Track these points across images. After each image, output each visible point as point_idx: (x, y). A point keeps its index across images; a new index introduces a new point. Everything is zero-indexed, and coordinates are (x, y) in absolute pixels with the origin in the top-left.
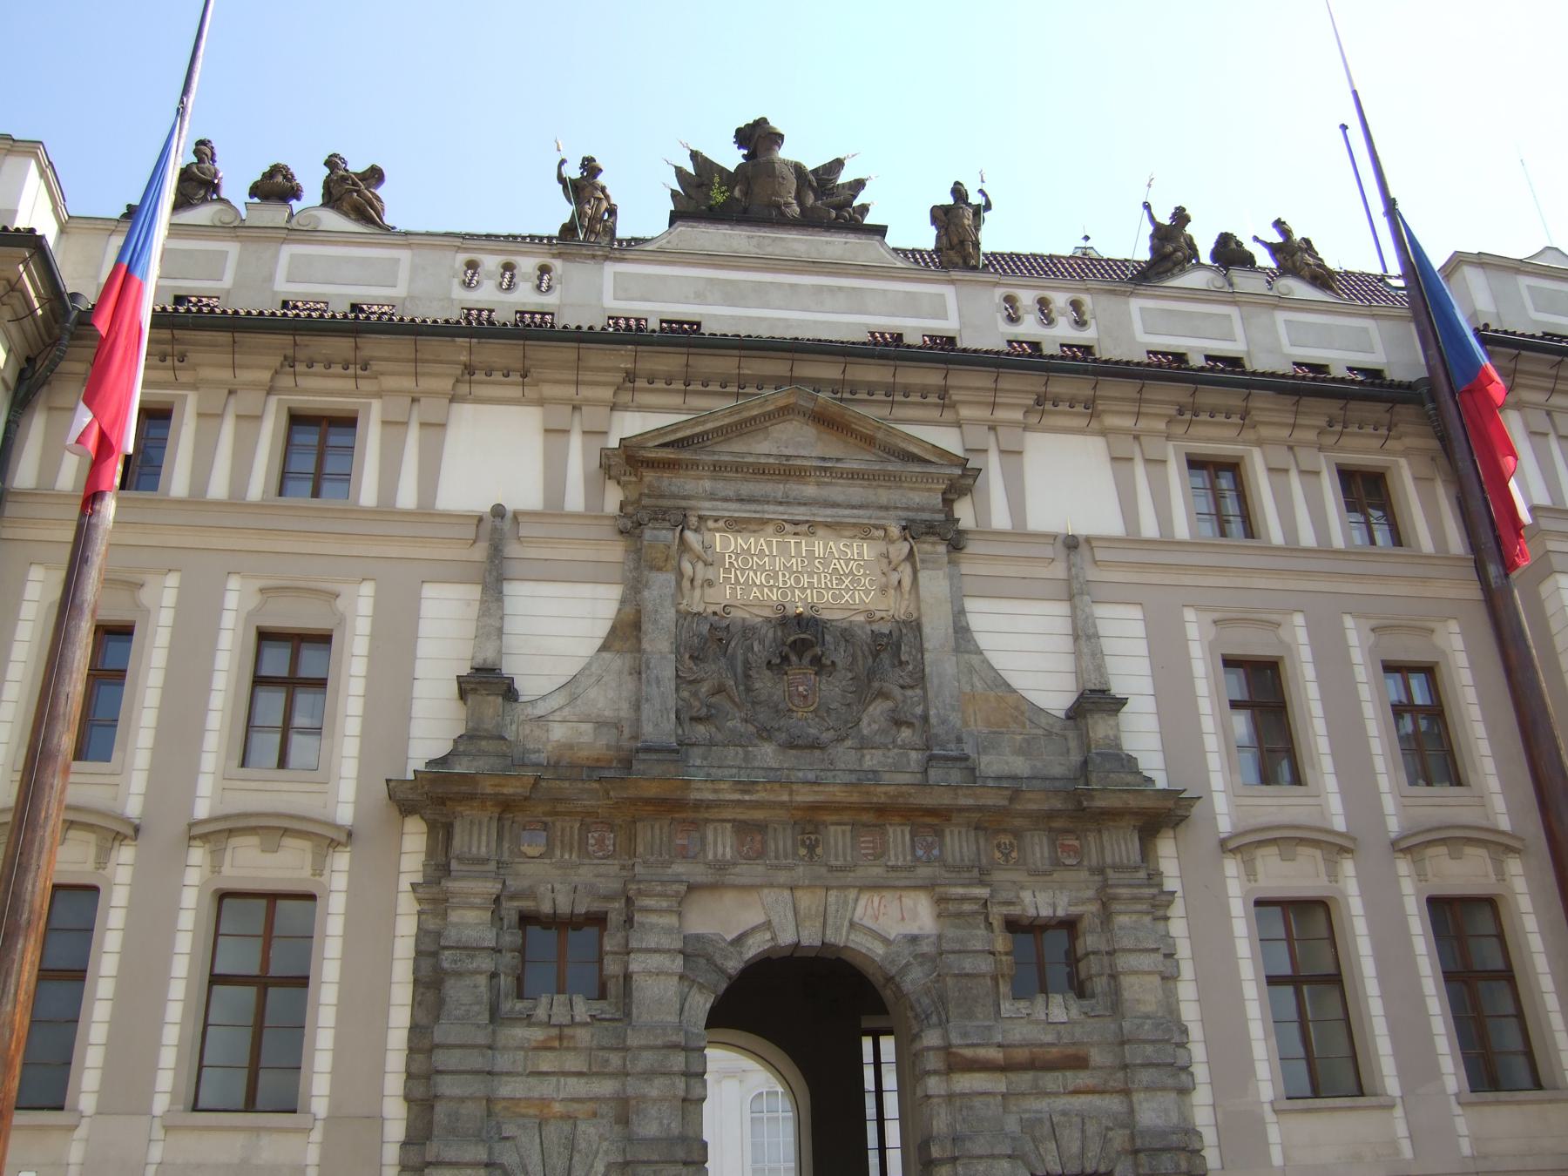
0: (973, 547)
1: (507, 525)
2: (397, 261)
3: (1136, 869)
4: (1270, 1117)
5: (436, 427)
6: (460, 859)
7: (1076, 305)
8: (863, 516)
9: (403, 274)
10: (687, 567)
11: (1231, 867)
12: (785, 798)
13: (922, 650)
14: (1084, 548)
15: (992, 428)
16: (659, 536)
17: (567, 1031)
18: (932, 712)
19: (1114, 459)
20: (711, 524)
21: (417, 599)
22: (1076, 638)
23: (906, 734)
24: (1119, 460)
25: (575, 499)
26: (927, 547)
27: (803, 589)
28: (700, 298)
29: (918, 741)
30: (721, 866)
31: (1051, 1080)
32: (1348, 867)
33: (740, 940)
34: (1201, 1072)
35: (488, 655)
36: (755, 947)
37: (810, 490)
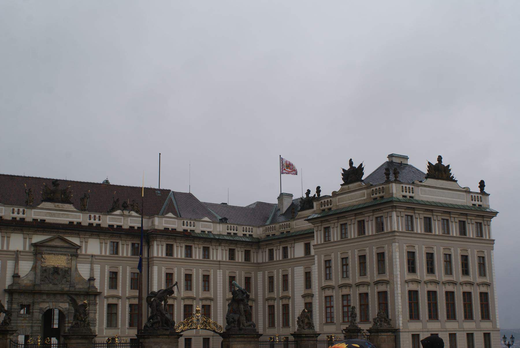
0: (79, 256)
1: (19, 253)
2: (2, 209)
3: (93, 300)
4: (104, 329)
5: (9, 237)
6: (14, 298)
7: (100, 216)
8: (66, 253)
9: (3, 211)
10: (42, 260)
11: (105, 300)
12: (53, 292)
13: (71, 272)
14: (94, 257)
15: (84, 238)
16: (39, 256)
17: (26, 318)
18: (71, 280)
19: (100, 243)
20: (46, 254)
21: (6, 263)
22: (91, 270)
23: (68, 283)
24: (101, 243)
25: (27, 249)
26: (73, 258)
27: (57, 263)
28: (46, 216)
29: (69, 284)
30: (44, 299)
32: (120, 300)
33: (46, 308)
34: (97, 324)
35: (16, 272)
36: (48, 309)
37: (59, 249)
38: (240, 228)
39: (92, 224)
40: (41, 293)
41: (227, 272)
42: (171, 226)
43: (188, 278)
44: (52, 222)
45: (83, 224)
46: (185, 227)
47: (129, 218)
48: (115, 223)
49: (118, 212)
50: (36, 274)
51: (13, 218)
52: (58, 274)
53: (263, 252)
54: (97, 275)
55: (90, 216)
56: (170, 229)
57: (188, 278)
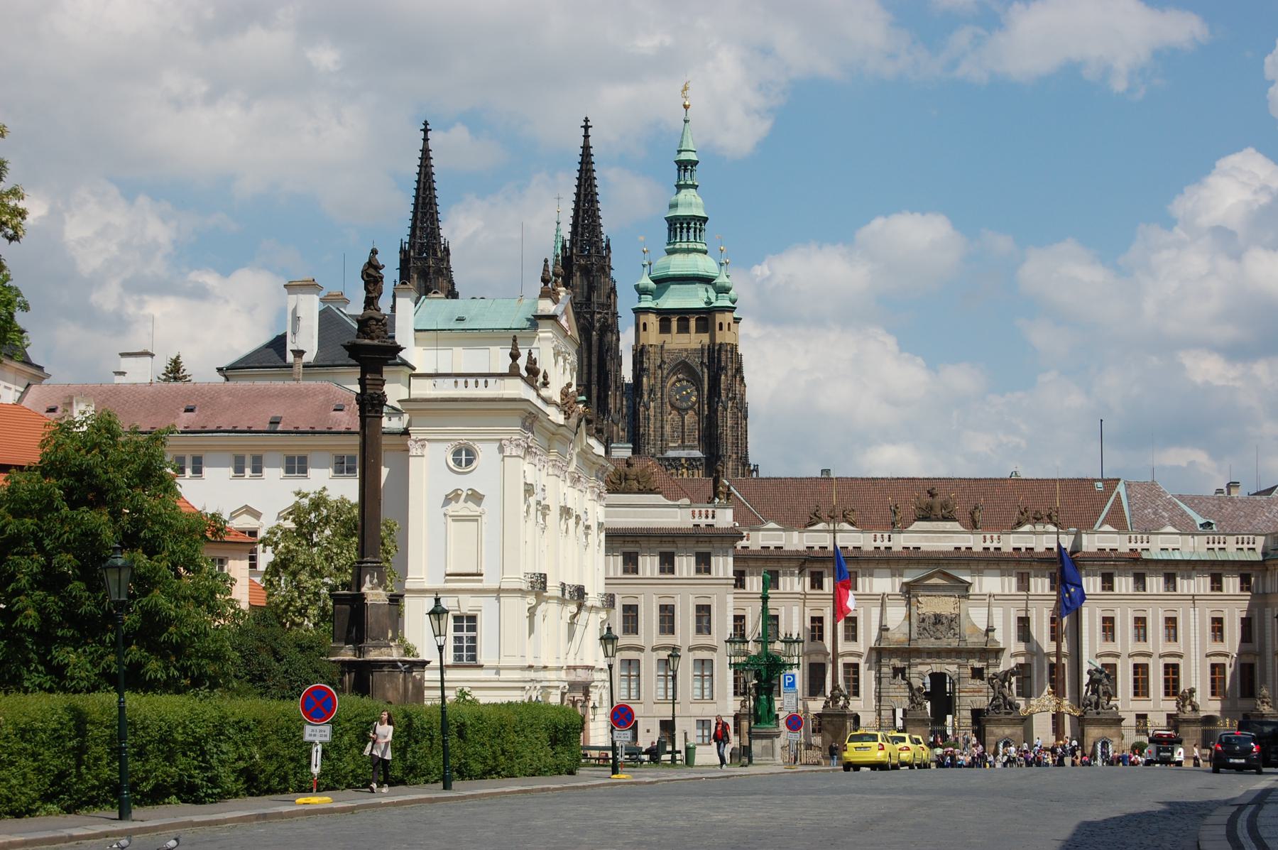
25: (897, 591)
31: (976, 694)
38: (1231, 540)
39: (989, 549)
40: (918, 653)
41: (1208, 611)
42: (1107, 546)
43: (1140, 623)
44: (929, 549)
45: (974, 550)
46: (1133, 545)
47: (1045, 536)
48: (1023, 546)
49: (1027, 528)
50: (910, 624)
51: (875, 548)
52: (942, 624)
53: (1271, 576)
54: (998, 623)
55: (985, 537)
56: (1108, 550)
57: (1140, 623)
